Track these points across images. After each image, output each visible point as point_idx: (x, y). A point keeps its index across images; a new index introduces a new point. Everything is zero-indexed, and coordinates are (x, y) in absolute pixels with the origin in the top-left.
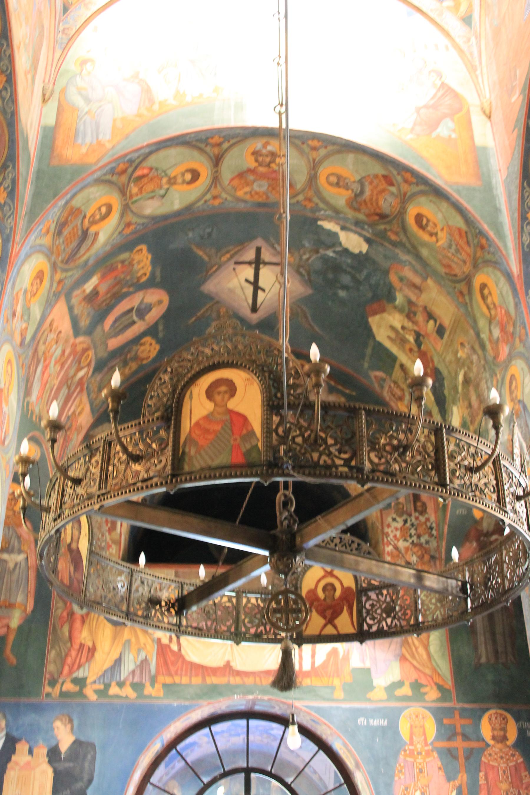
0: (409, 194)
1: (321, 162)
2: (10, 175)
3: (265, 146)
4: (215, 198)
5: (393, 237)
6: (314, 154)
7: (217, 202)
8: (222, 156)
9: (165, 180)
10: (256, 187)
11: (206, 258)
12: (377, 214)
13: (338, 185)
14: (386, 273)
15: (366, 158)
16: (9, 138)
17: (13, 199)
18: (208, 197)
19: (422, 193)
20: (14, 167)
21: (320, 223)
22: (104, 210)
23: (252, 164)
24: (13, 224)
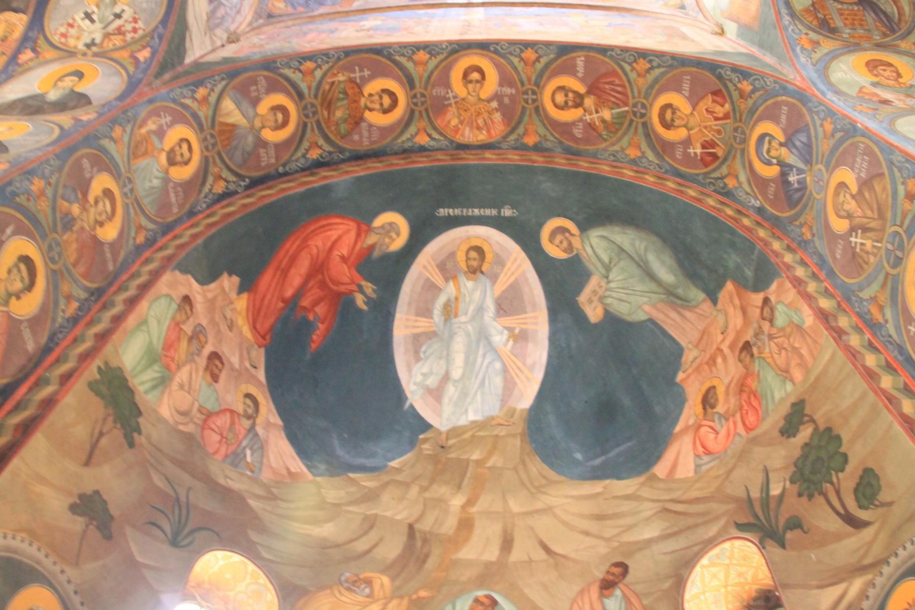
2: (728, 73)
16: (693, 66)
17: (750, 75)
20: (722, 68)
24: (771, 79)
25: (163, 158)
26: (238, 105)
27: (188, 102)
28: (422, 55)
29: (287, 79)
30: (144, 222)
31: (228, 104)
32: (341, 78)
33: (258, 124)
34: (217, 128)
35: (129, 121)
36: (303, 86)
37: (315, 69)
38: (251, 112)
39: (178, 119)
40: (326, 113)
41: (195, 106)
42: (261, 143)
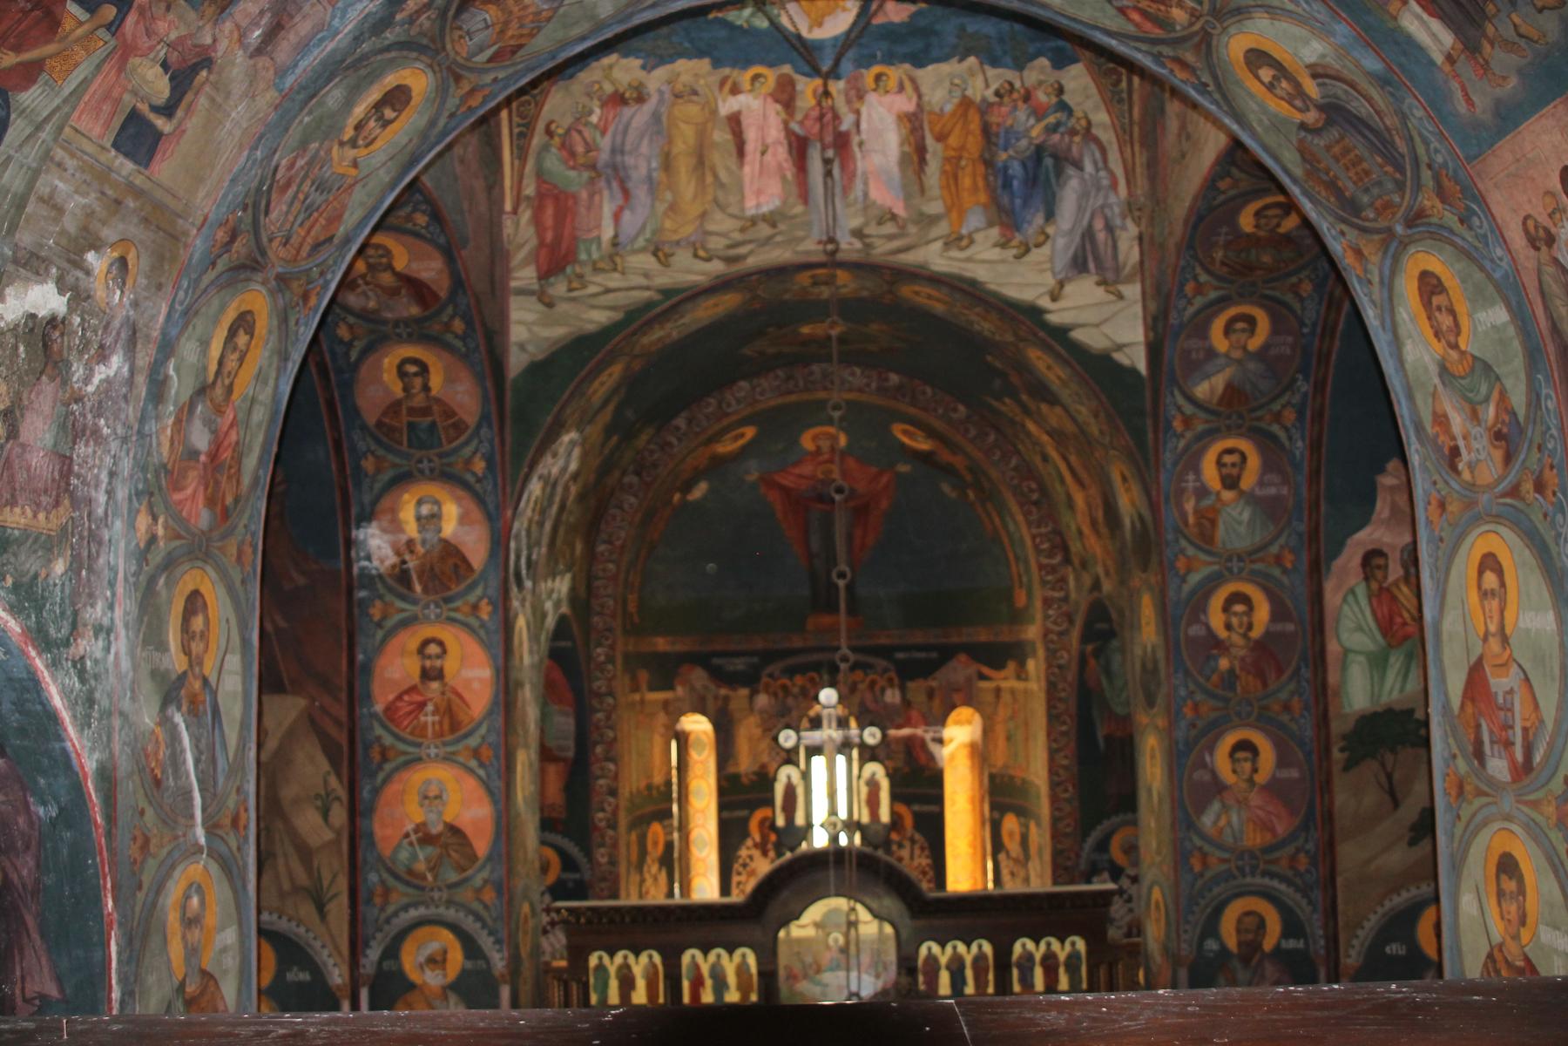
19: (432, 123)
22: (1266, 74)
25: (1227, 495)
26: (1208, 377)
27: (1182, 444)
30: (1274, 549)
31: (1202, 390)
33: (1237, 354)
34: (1221, 409)
35: (1177, 541)
36: (1213, 295)
38: (1221, 361)
40: (1259, 272)
41: (1189, 435)
42: (1262, 354)
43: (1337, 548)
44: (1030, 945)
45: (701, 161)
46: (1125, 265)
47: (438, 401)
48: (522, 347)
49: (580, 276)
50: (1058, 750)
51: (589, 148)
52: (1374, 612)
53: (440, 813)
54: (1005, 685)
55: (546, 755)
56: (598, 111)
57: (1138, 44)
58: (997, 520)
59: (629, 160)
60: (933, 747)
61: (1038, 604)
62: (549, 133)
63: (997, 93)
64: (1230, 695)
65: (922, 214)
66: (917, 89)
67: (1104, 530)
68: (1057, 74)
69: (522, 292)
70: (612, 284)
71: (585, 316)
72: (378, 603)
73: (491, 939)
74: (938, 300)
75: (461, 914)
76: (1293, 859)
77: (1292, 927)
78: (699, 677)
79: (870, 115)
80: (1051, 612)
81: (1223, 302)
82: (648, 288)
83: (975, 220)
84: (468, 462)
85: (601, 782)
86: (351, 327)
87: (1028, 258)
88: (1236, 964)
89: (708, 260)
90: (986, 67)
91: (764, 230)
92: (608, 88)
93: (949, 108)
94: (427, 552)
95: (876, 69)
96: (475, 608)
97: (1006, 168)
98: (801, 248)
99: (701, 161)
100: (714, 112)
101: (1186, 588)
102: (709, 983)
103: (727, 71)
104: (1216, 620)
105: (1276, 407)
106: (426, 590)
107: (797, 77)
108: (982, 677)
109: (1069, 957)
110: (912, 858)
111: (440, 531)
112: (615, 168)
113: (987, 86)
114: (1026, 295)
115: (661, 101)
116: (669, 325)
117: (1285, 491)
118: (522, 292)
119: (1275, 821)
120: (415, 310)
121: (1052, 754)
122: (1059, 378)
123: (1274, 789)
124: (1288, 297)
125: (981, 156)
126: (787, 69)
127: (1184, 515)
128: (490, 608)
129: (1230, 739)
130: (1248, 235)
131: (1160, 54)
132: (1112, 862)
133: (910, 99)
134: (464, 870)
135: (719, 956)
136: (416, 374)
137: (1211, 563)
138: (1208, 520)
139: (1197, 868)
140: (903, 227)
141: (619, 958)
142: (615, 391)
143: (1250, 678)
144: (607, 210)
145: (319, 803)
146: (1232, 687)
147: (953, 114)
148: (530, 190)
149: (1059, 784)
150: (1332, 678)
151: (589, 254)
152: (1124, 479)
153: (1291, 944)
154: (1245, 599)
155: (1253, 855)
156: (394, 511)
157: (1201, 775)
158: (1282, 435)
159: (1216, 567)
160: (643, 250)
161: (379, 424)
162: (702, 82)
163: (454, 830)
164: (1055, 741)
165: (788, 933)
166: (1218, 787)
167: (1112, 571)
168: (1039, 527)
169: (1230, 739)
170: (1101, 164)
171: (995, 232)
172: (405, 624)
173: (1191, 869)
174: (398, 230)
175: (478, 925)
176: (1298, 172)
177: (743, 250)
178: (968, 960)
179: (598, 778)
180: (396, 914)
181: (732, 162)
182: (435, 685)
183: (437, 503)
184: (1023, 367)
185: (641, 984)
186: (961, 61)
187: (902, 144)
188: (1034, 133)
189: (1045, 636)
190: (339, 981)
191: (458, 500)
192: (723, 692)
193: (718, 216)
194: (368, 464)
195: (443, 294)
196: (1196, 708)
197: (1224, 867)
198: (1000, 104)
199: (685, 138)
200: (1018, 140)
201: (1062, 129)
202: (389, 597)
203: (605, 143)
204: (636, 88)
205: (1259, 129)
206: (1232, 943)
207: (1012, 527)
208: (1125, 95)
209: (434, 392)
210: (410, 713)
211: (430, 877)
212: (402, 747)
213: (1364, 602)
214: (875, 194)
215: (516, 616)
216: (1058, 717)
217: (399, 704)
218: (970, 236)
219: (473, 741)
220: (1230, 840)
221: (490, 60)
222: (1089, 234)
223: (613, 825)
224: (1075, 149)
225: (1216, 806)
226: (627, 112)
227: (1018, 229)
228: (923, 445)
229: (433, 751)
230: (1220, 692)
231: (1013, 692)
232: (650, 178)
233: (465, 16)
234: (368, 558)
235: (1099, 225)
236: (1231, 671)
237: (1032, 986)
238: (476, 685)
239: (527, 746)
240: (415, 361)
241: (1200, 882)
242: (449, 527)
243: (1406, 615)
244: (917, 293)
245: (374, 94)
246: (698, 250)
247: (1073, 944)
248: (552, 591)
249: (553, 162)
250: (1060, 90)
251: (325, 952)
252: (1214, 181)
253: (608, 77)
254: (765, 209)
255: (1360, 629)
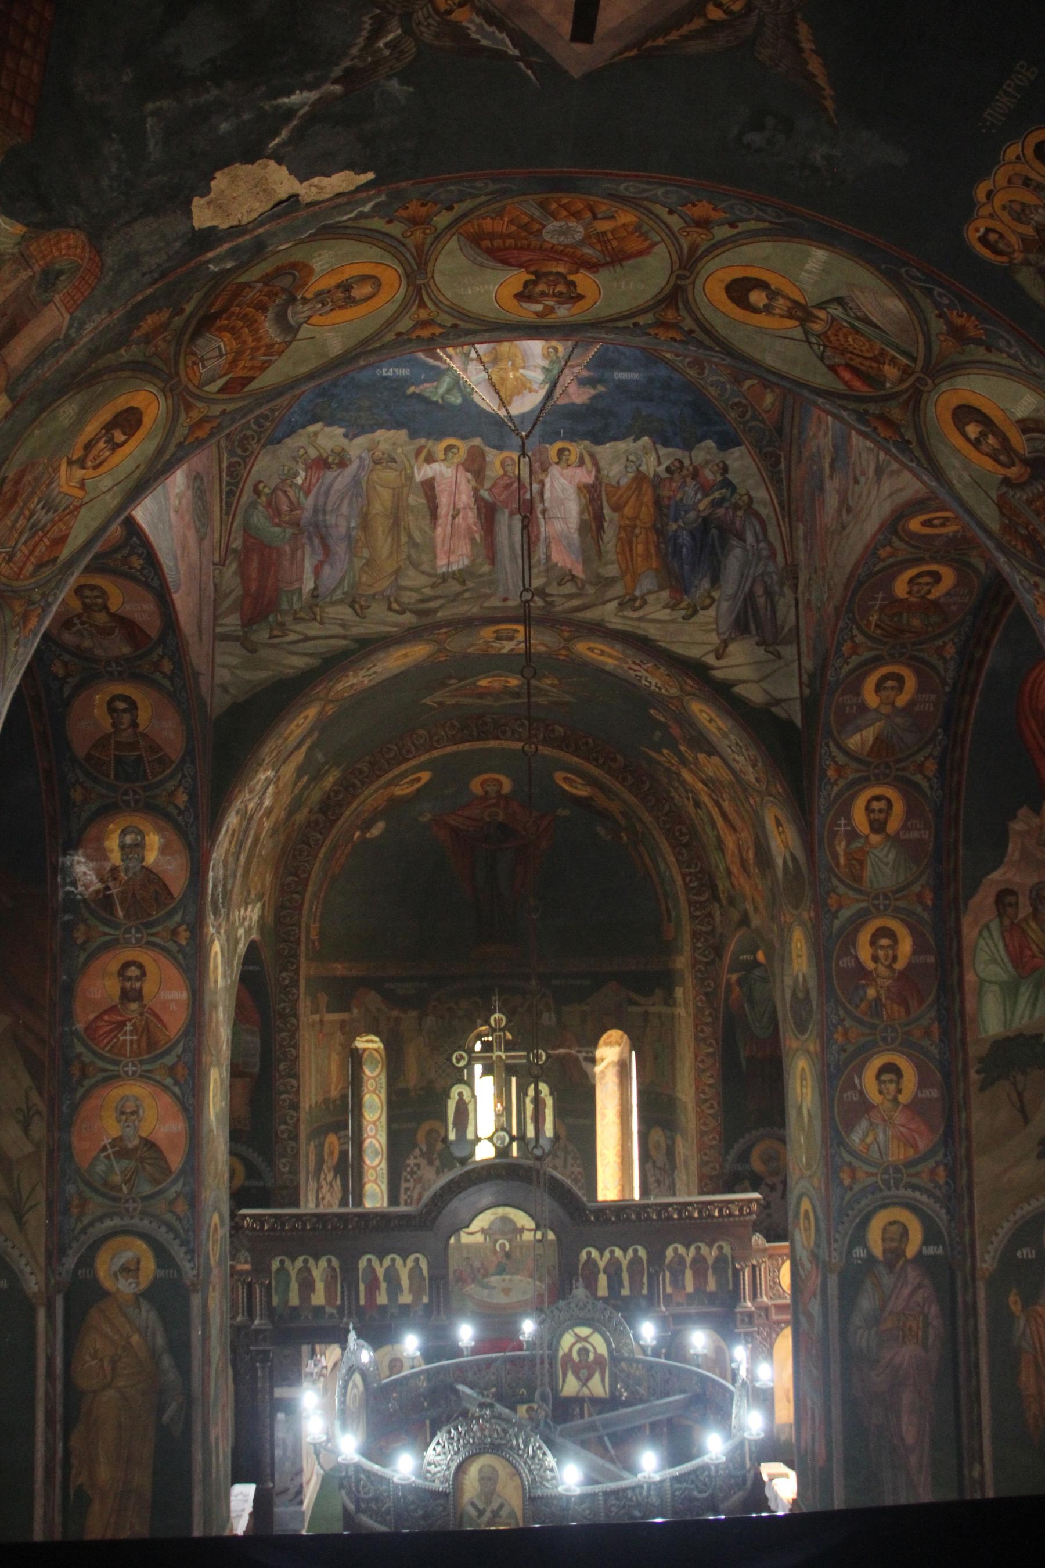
0: (183, 416)
1: (404, 307)
3: (551, 310)
4: (704, 224)
5: (151, 321)
6: (423, 314)
7: (702, 209)
8: (660, 302)
9: (817, 327)
10: (578, 230)
11: (804, 31)
12: (218, 315)
13: (346, 287)
14: (97, 234)
15: (303, 370)
18: (722, 232)
19: (160, 451)
21: (371, 176)
22: (973, 430)
23: (583, 280)
25: (875, 838)
26: (859, 729)
27: (836, 789)
28: (882, 553)
29: (851, 672)
30: (916, 888)
32: (874, 618)
33: (885, 710)
36: (867, 655)
37: (853, 641)
39: (846, 810)
40: (909, 635)
41: (841, 783)
43: (973, 888)
44: (681, 1250)
45: (396, 522)
46: (783, 628)
47: (145, 736)
48: (225, 688)
49: (282, 625)
50: (704, 1071)
51: (294, 506)
52: (1006, 946)
53: (136, 1128)
54: (653, 1009)
55: (236, 1072)
56: (303, 474)
57: (844, 403)
58: (647, 861)
59: (331, 520)
60: (586, 1065)
61: (687, 937)
62: (257, 492)
63: (668, 470)
64: (876, 1021)
65: (599, 576)
66: (596, 464)
67: (754, 870)
68: (722, 455)
69: (225, 637)
70: (312, 633)
71: (285, 662)
72: (82, 927)
73: (183, 1249)
74: (610, 656)
75: (154, 1225)
76: (933, 1172)
77: (931, 1236)
78: (373, 999)
79: (552, 486)
80: (699, 945)
81: (876, 661)
82: (344, 637)
83: (647, 583)
84: (172, 794)
85: (283, 1097)
86: (65, 664)
87: (694, 619)
88: (882, 1269)
89: (402, 612)
90: (658, 446)
91: (454, 587)
92: (313, 453)
93: (624, 482)
94: (130, 879)
95: (559, 445)
96: (174, 933)
97: (676, 537)
98: (486, 605)
99: (396, 522)
100: (411, 478)
101: (837, 923)
102: (383, 1286)
103: (423, 441)
104: (864, 953)
105: (919, 758)
106: (127, 916)
107: (487, 449)
108: (632, 1002)
109: (717, 1260)
110: (565, 1166)
111: (143, 860)
112: (316, 526)
113: (660, 464)
114: (694, 653)
115: (361, 466)
116: (362, 673)
117: (925, 835)
118: (225, 637)
119: (917, 1137)
120: (126, 650)
121: (699, 1072)
122: (719, 729)
123: (915, 1107)
124: (934, 660)
125: (654, 526)
126: (477, 441)
127: (835, 856)
128: (188, 934)
129: (877, 1062)
130: (902, 600)
131: (866, 412)
132: (752, 1172)
133: (589, 472)
134: (159, 1183)
135: (393, 1260)
136: (124, 711)
137: (858, 901)
138: (857, 860)
139: (847, 1182)
140: (582, 588)
141: (299, 1262)
142: (309, 733)
143: (895, 1007)
144: (308, 565)
145: (21, 1117)
146: (879, 1015)
147: (629, 487)
148: (237, 544)
149: (706, 1101)
150: (970, 1006)
151: (290, 603)
152: (778, 823)
153: (931, 1250)
154: (891, 934)
155: (897, 1170)
156: (100, 839)
157: (851, 1096)
158: (924, 784)
159: (864, 905)
160: (341, 601)
161: (89, 757)
162: (399, 450)
163: (149, 1144)
164: (702, 1061)
165: (458, 1240)
166: (865, 1107)
167: (761, 907)
168: (688, 867)
169: (877, 1062)
170: (761, 537)
171: (665, 594)
172: (107, 947)
173: (841, 1183)
174: (114, 572)
175: (171, 1236)
176: (995, 526)
177: (433, 605)
178: (625, 1263)
179: (281, 1093)
180: (92, 1224)
181: (425, 523)
182: (134, 1006)
183: (140, 832)
184: (686, 721)
185: (320, 1286)
186: (635, 441)
187: (581, 513)
188: (701, 507)
189: (694, 966)
190: (36, 1288)
191: (160, 831)
192: (395, 1013)
193: (412, 572)
194: (77, 795)
195: (154, 634)
196: (845, 1034)
197: (871, 1180)
198: (671, 479)
199: (382, 502)
200: (686, 512)
201: (726, 504)
202: (93, 922)
203: (309, 502)
204: (338, 454)
205: (958, 486)
206: (878, 1251)
207: (662, 867)
208: (783, 476)
209: (141, 728)
210: (111, 1031)
211: (124, 1188)
212: (100, 1064)
213: (996, 934)
214: (555, 557)
215: (212, 942)
216: (704, 1039)
217: (100, 1023)
218: (643, 597)
219: (169, 1060)
220: (877, 1155)
221: (221, 390)
222: (750, 596)
223: (295, 1138)
224: (738, 523)
225: (864, 1124)
226: (330, 475)
227: (686, 592)
228: (583, 792)
229: (130, 1069)
230: (866, 1019)
231: (660, 1016)
232: (349, 537)
233: (200, 341)
234: (74, 883)
235: (759, 590)
236: (877, 999)
237: (684, 1287)
238: (173, 1007)
239: (219, 1065)
240: (126, 698)
241: (848, 1197)
242: (151, 857)
243: (1034, 947)
244: (591, 649)
245: (106, 415)
246: (389, 603)
247: (720, 1248)
248: (244, 919)
249: (260, 519)
250: (725, 469)
251: (23, 1261)
252: (876, 548)
253: (312, 444)
254: (455, 568)
255: (994, 961)
